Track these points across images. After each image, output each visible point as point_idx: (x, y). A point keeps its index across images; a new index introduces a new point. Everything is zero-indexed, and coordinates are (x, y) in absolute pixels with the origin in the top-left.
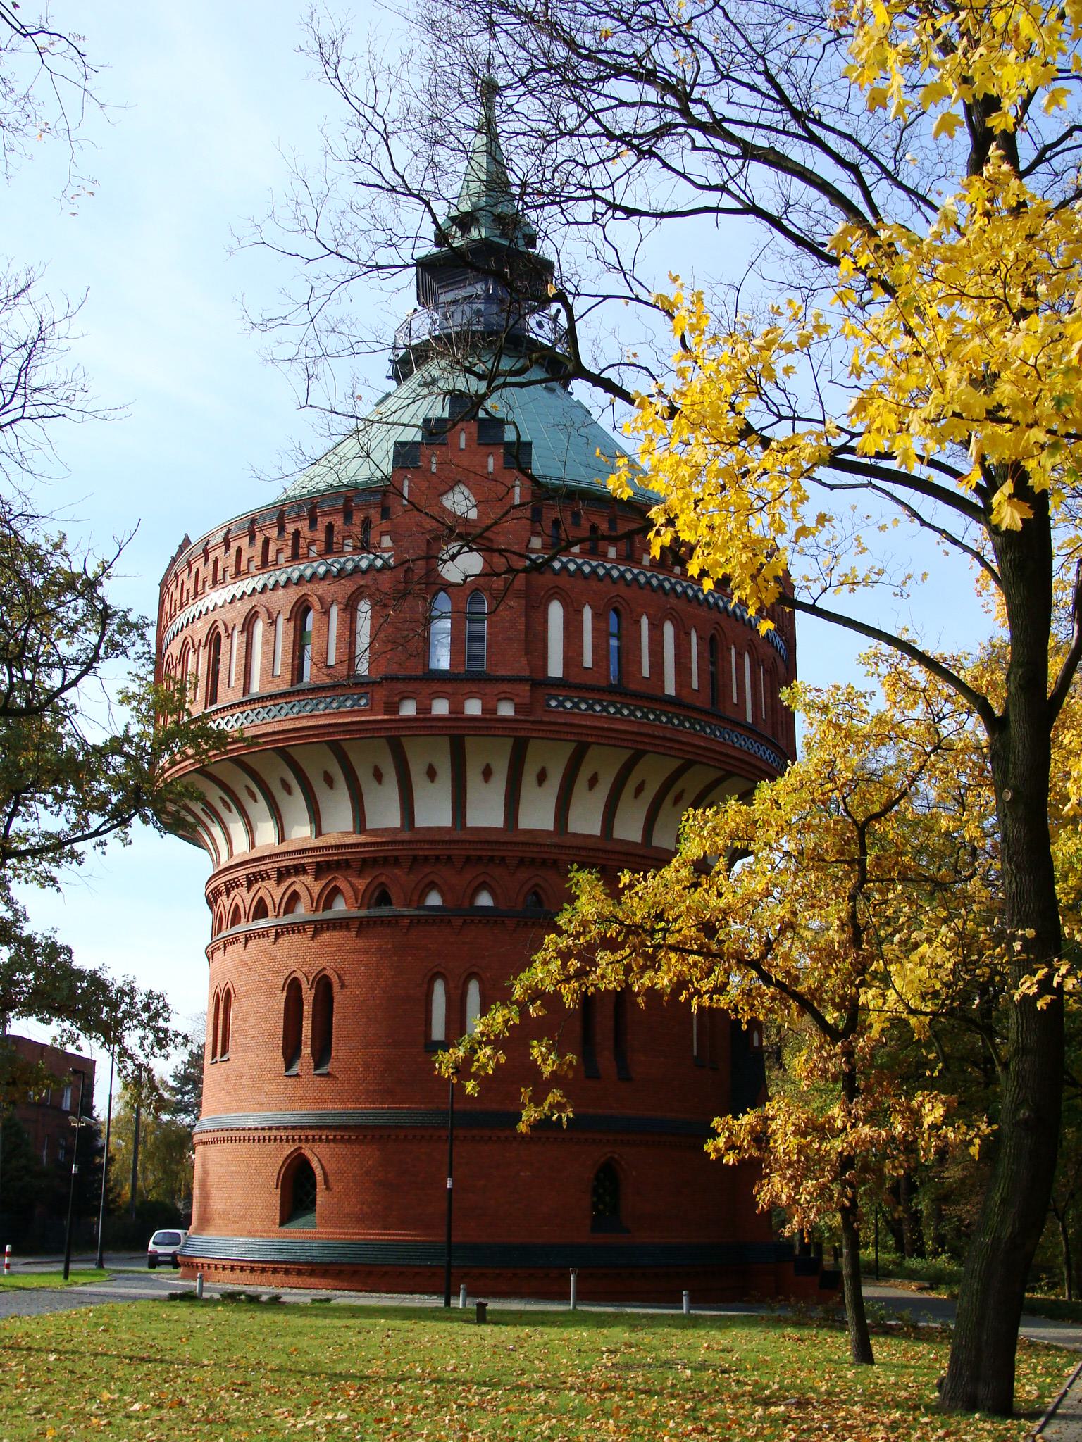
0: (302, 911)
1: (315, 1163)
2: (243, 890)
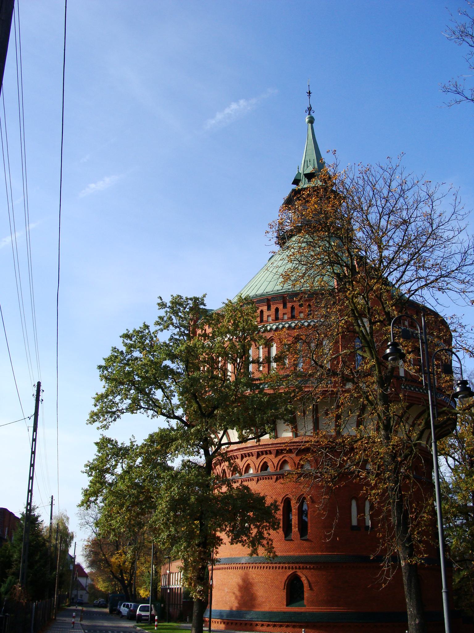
0: (288, 468)
1: (303, 579)
2: (254, 458)
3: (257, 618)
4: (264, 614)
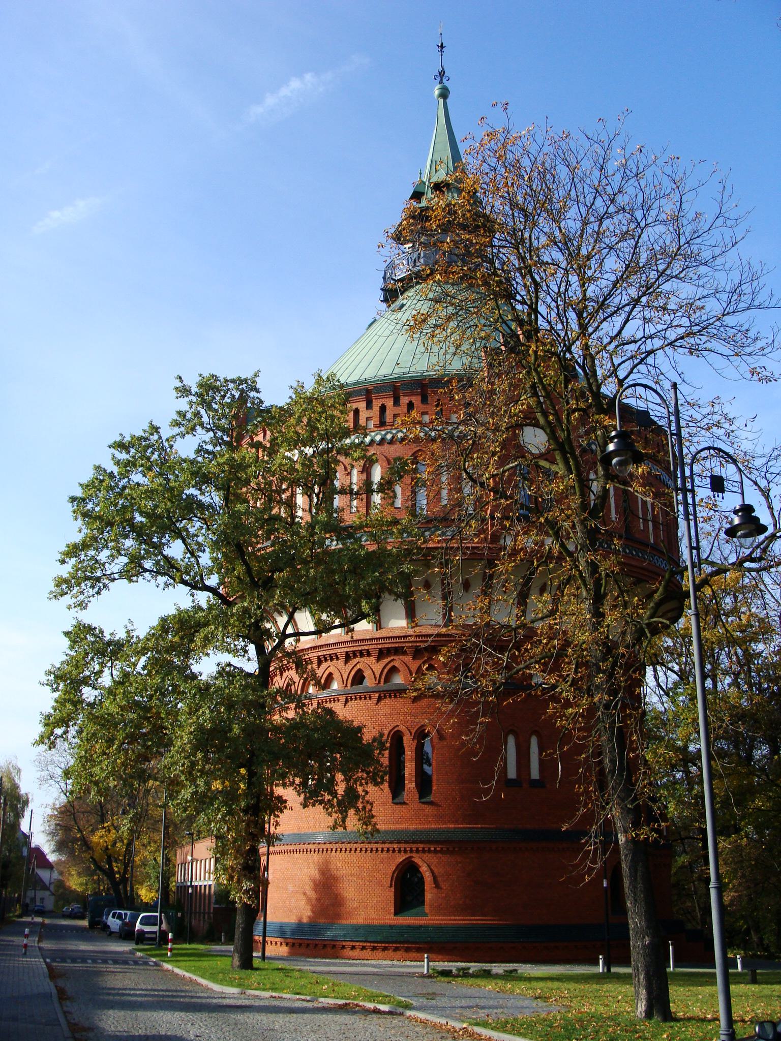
0: (398, 680)
1: (424, 869)
2: (341, 663)
3: (345, 936)
4: (357, 928)
